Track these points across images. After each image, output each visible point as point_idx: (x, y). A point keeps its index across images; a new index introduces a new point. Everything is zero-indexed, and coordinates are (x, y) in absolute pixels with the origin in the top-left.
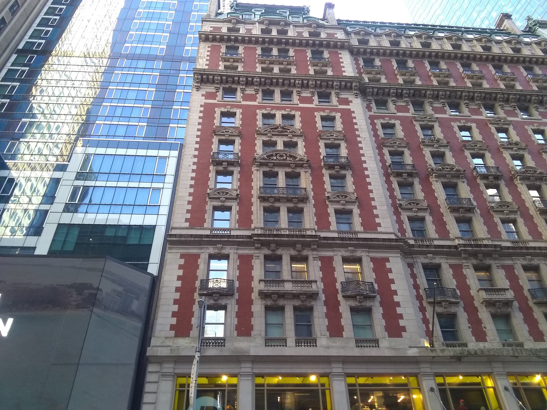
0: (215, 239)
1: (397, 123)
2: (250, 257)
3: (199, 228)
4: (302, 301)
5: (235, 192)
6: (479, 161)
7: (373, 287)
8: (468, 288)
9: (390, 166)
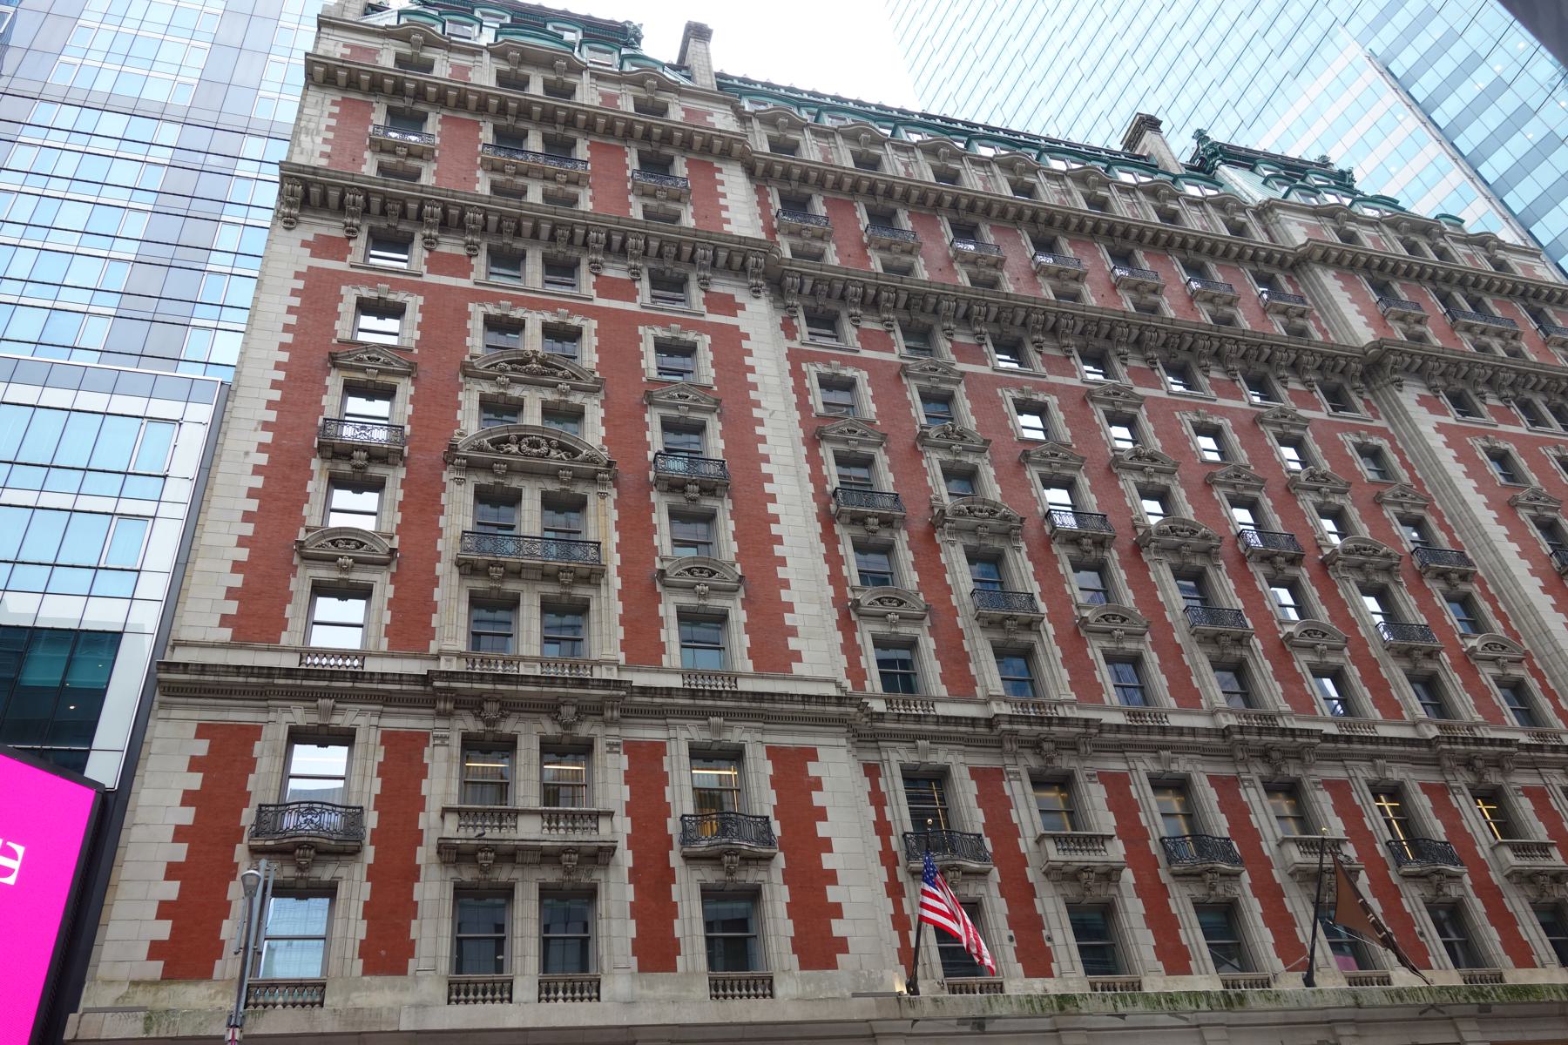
0: (312, 683)
1: (862, 377)
2: (421, 739)
3: (265, 645)
4: (568, 872)
5: (386, 541)
6: (1058, 496)
7: (769, 830)
8: (1014, 832)
9: (835, 494)
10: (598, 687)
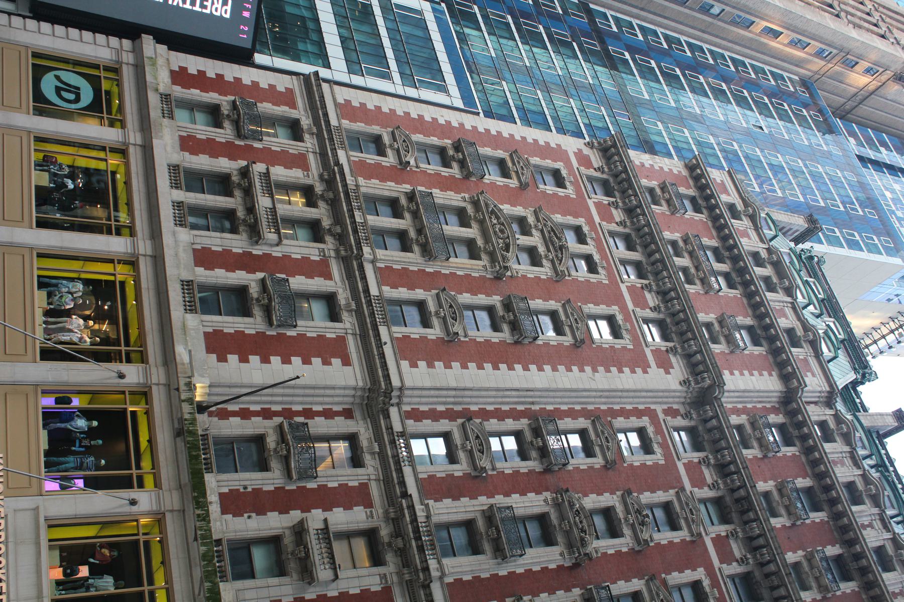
2: (306, 167)
3: (339, 112)
10: (355, 240)
